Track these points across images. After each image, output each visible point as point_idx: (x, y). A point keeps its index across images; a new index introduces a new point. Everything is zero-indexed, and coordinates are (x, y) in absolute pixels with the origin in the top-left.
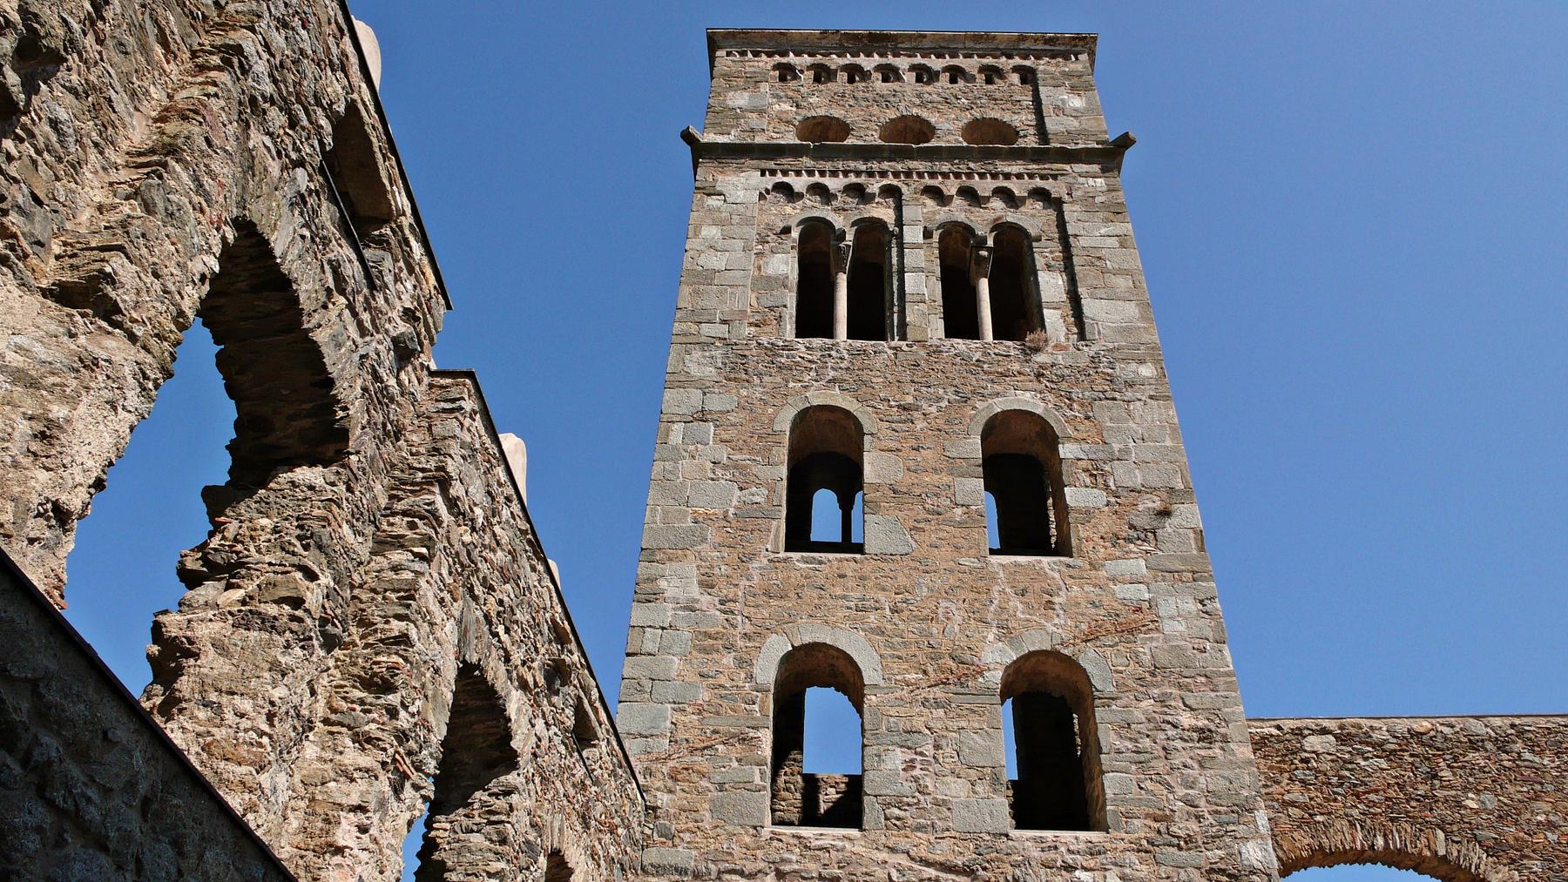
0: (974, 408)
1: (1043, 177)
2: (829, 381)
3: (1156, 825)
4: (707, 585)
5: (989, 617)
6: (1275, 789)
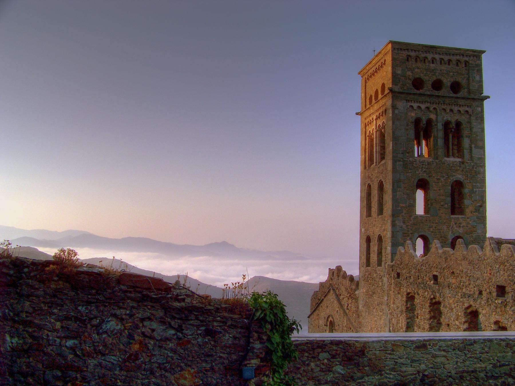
0: (450, 179)
1: (468, 106)
4: (404, 222)
5: (450, 229)
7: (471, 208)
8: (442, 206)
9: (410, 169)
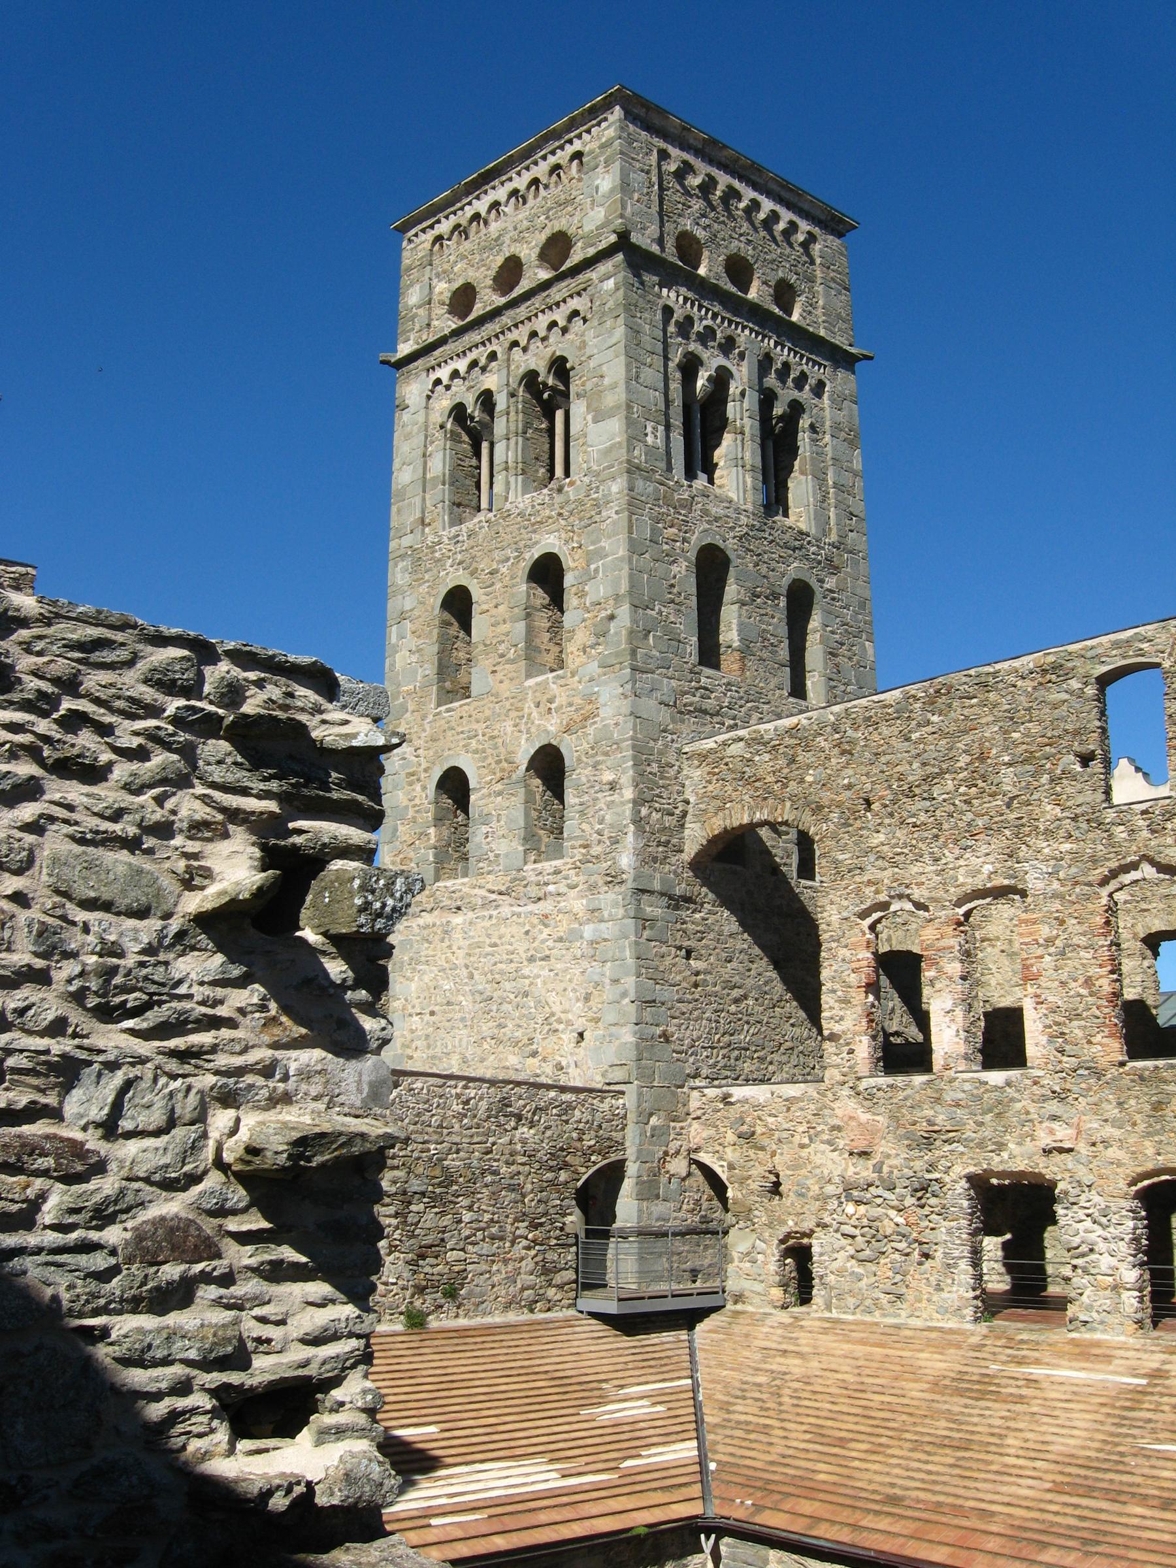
3: (584, 851)
6: (710, 788)
8: (502, 656)
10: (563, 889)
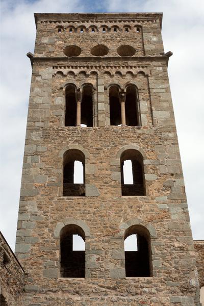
0: (118, 149)
1: (143, 67)
2: (75, 141)
3: (166, 275)
4: (40, 207)
7: (156, 185)
9: (53, 139)
10: (154, 291)
